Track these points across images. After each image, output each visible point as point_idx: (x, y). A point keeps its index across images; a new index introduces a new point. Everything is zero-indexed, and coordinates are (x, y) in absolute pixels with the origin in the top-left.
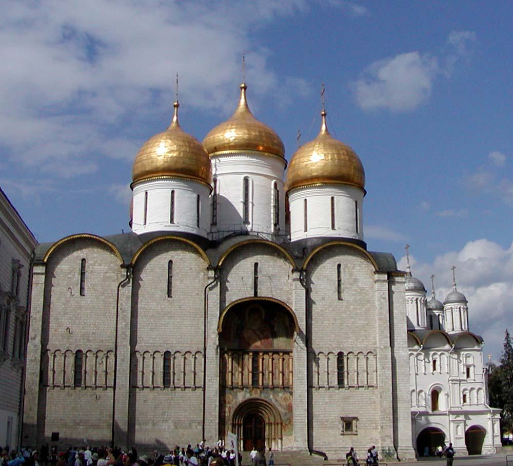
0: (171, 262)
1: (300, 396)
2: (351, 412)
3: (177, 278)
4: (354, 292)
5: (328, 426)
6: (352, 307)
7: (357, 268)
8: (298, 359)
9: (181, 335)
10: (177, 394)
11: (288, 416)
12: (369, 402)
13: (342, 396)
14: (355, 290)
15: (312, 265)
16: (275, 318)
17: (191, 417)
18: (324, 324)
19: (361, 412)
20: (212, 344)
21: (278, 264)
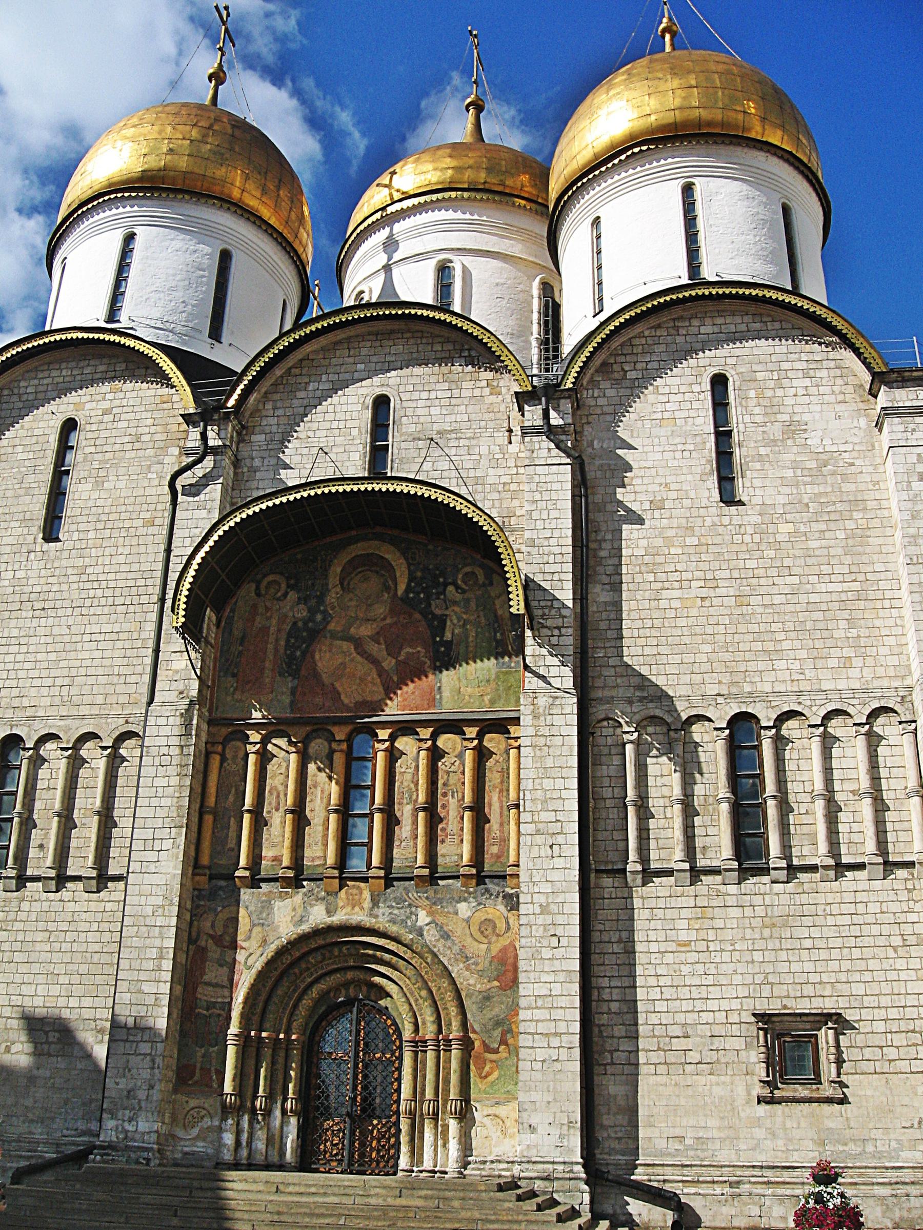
0: (70, 426)
1: (544, 909)
2: (808, 990)
3: (82, 474)
4: (790, 473)
5: (693, 1057)
6: (784, 528)
7: (795, 383)
8: (542, 741)
9: (74, 672)
10: (25, 906)
11: (497, 1010)
12: (897, 941)
13: (760, 911)
14: (795, 466)
15: (605, 384)
16: (451, 588)
17: (73, 1002)
18: (663, 604)
19: (859, 989)
20: (172, 696)
21: (465, 393)
